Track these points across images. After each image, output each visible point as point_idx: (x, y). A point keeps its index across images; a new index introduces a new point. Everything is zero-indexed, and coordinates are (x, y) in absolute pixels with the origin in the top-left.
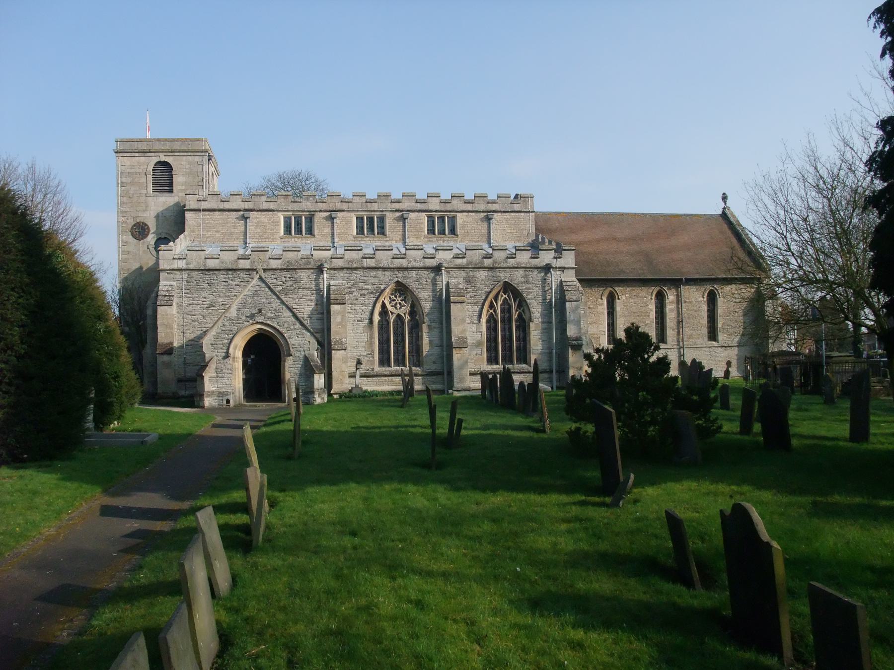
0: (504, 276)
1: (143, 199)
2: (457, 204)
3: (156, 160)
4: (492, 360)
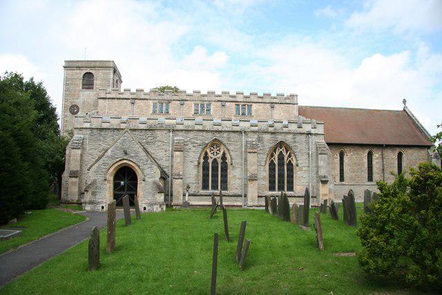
0: (280, 138)
1: (76, 93)
2: (254, 99)
3: (85, 72)
4: (272, 188)
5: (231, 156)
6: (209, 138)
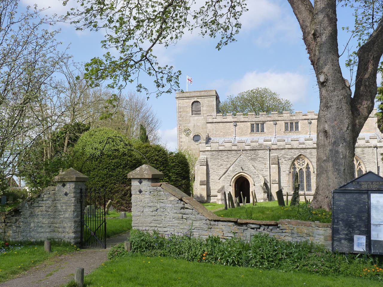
1: (188, 118)
3: (193, 100)
5: (313, 166)
6: (297, 153)
